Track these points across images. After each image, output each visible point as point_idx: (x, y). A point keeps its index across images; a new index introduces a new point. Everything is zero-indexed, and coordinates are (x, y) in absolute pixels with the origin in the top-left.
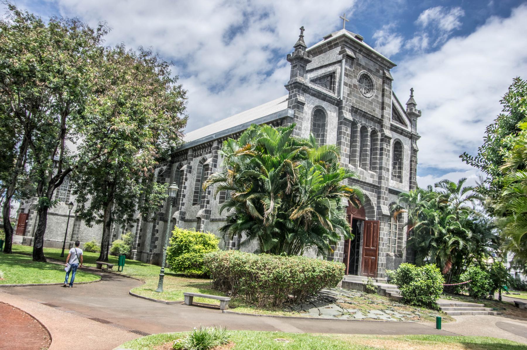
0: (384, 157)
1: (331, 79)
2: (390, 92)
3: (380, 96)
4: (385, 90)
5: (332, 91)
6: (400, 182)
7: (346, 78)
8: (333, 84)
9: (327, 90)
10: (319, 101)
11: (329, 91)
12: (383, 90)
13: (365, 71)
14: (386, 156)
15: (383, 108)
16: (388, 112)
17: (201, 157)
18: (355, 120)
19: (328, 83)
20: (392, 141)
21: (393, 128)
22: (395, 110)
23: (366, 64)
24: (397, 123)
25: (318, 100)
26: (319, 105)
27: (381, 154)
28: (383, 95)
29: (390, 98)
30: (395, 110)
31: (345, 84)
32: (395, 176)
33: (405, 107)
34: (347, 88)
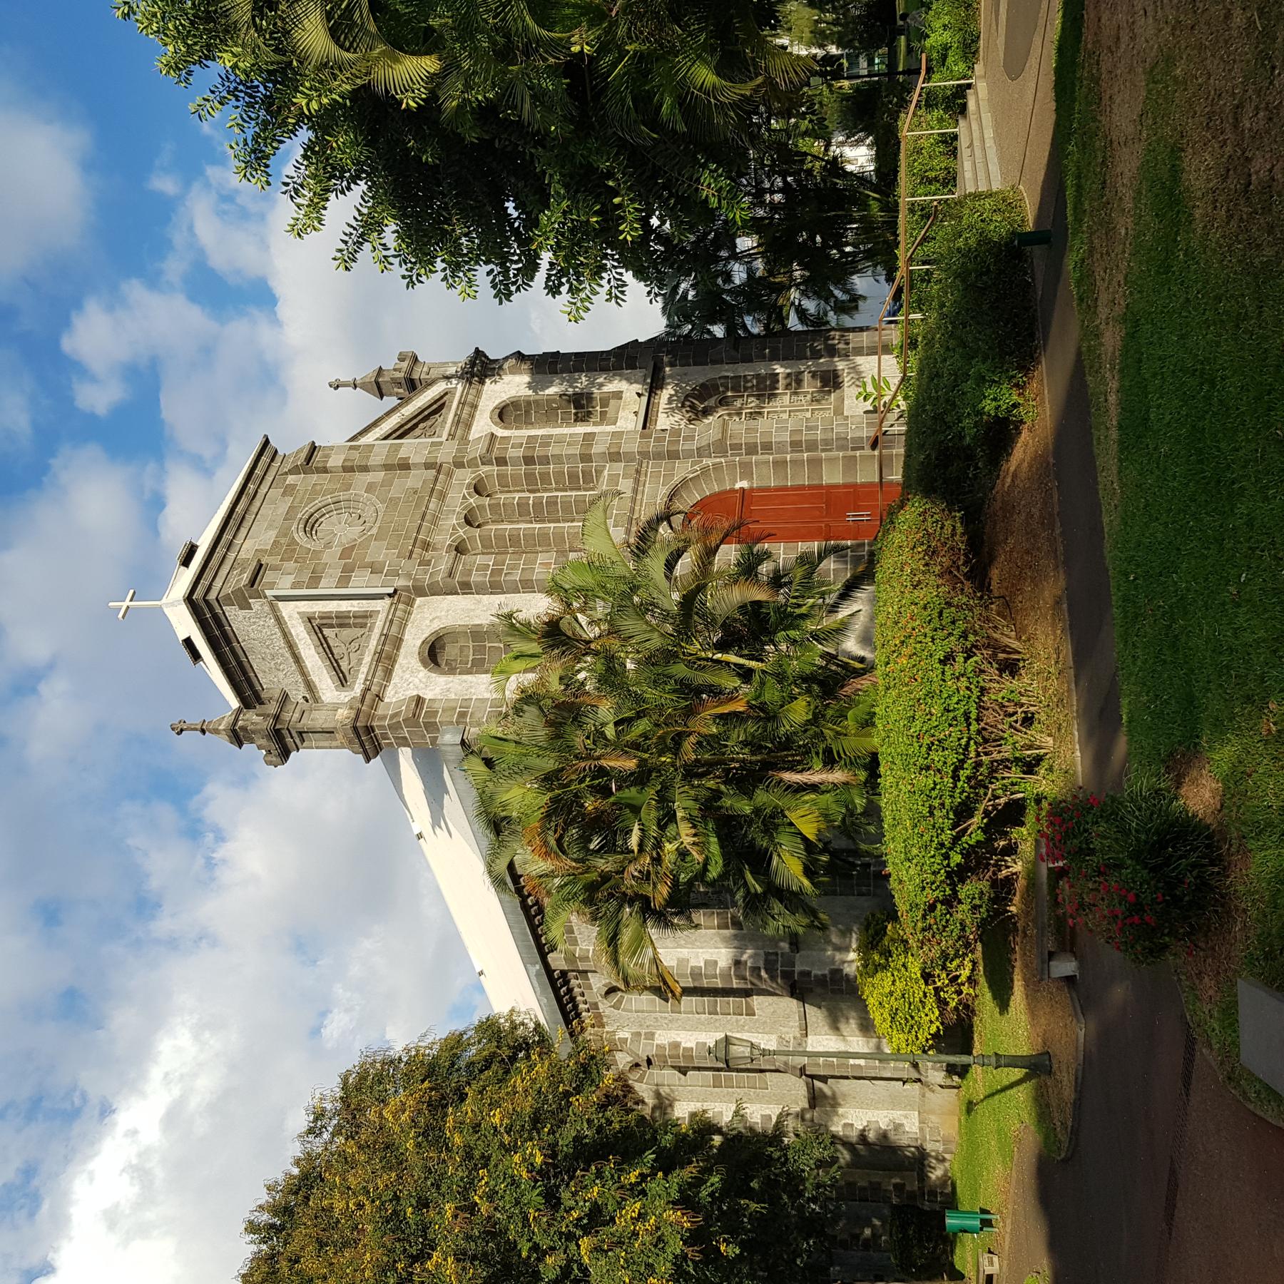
0: (552, 450)
1: (331, 626)
2: (351, 448)
3: (369, 477)
4: (349, 464)
5: (369, 621)
6: (621, 398)
7: (323, 582)
8: (347, 621)
9: (369, 636)
10: (405, 657)
11: (371, 630)
12: (348, 469)
13: (294, 527)
14: (548, 444)
15: (405, 466)
16: (412, 448)
17: (600, 1005)
18: (450, 545)
19: (346, 633)
20: (500, 432)
21: (459, 432)
22: (402, 432)
23: (269, 527)
24: (444, 422)
25: (401, 660)
26: (416, 656)
27: (545, 460)
28: (365, 469)
29: (370, 447)
30: (402, 432)
31: (344, 581)
32: (603, 414)
33: (391, 401)
34: (354, 580)
